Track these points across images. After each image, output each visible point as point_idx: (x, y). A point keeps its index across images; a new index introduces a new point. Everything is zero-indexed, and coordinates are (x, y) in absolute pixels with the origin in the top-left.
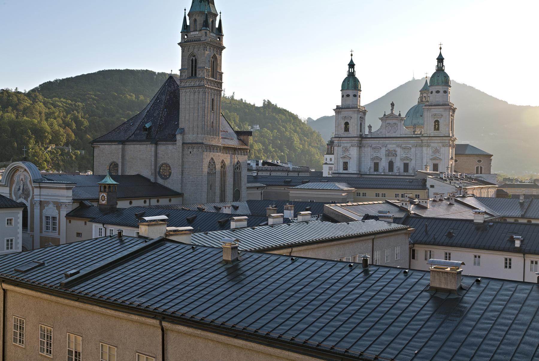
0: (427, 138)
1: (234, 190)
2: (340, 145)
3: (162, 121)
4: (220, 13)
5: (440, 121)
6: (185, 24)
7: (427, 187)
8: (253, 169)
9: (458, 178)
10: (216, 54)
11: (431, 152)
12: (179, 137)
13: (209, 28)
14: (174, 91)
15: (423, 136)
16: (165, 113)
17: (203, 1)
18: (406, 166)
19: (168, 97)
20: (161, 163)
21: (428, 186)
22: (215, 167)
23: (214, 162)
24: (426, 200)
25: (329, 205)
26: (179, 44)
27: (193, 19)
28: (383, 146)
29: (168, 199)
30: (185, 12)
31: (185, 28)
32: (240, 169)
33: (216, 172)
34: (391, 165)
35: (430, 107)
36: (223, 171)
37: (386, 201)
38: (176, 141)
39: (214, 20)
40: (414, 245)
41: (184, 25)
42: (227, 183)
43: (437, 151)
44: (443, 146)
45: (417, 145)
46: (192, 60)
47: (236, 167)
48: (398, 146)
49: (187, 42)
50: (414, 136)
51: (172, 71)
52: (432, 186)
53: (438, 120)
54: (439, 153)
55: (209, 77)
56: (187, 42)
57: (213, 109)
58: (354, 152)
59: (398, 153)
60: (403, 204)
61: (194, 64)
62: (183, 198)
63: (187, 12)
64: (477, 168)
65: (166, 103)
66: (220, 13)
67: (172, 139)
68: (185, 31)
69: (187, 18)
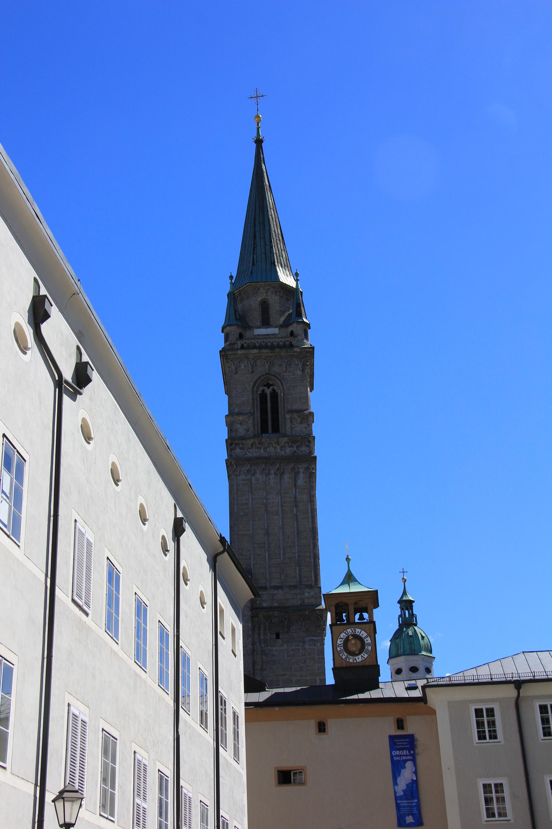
27: (259, 299)
31: (238, 317)
46: (263, 396)
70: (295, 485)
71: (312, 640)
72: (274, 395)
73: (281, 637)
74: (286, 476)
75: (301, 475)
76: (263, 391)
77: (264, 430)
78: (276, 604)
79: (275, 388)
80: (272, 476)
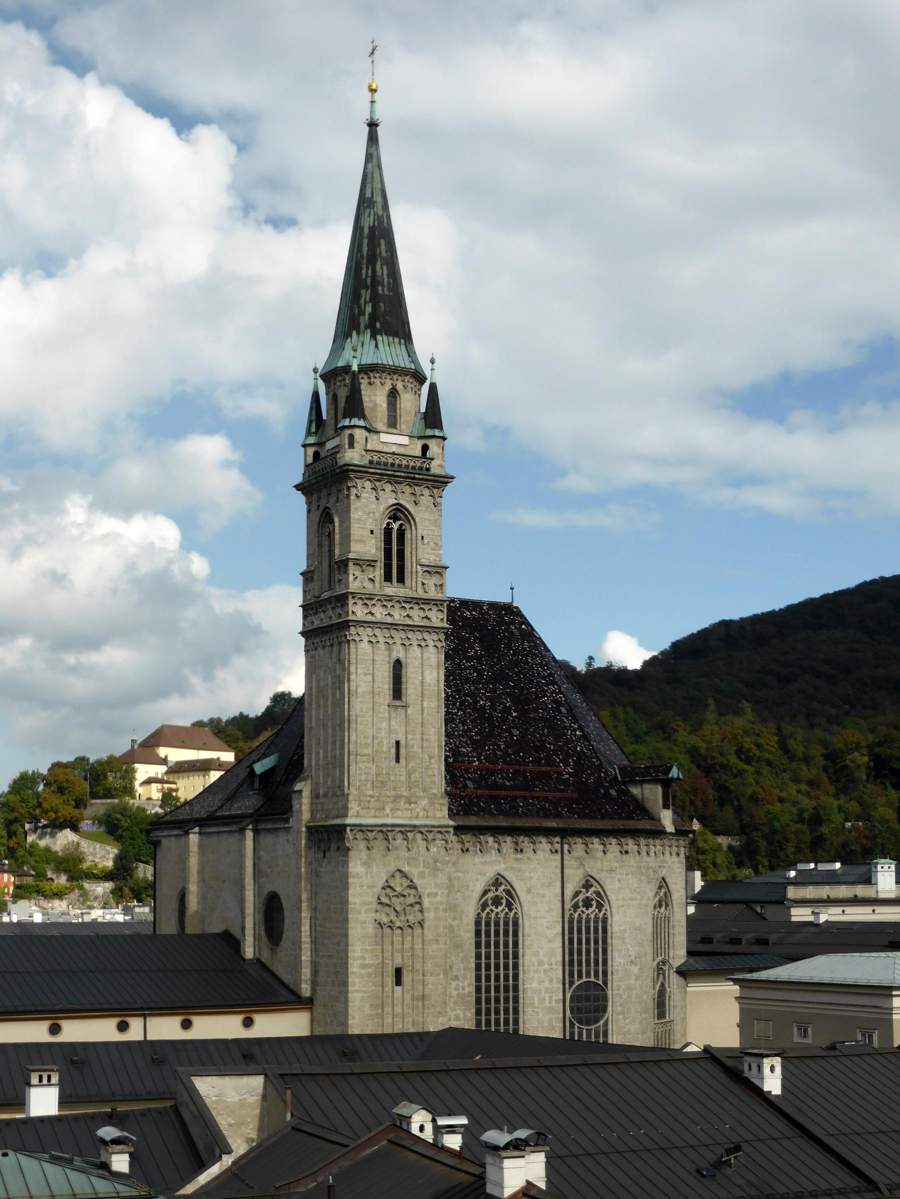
4: (432, 361)
8: (882, 896)
13: (363, 416)
17: (354, 334)
20: (266, 893)
23: (412, 886)
26: (298, 487)
29: (237, 1020)
31: (313, 429)
32: (600, 906)
36: (502, 915)
39: (400, 386)
42: (618, 959)
47: (581, 897)
57: (397, 692)
62: (312, 1014)
66: (432, 361)
68: (312, 440)
74: (335, 648)
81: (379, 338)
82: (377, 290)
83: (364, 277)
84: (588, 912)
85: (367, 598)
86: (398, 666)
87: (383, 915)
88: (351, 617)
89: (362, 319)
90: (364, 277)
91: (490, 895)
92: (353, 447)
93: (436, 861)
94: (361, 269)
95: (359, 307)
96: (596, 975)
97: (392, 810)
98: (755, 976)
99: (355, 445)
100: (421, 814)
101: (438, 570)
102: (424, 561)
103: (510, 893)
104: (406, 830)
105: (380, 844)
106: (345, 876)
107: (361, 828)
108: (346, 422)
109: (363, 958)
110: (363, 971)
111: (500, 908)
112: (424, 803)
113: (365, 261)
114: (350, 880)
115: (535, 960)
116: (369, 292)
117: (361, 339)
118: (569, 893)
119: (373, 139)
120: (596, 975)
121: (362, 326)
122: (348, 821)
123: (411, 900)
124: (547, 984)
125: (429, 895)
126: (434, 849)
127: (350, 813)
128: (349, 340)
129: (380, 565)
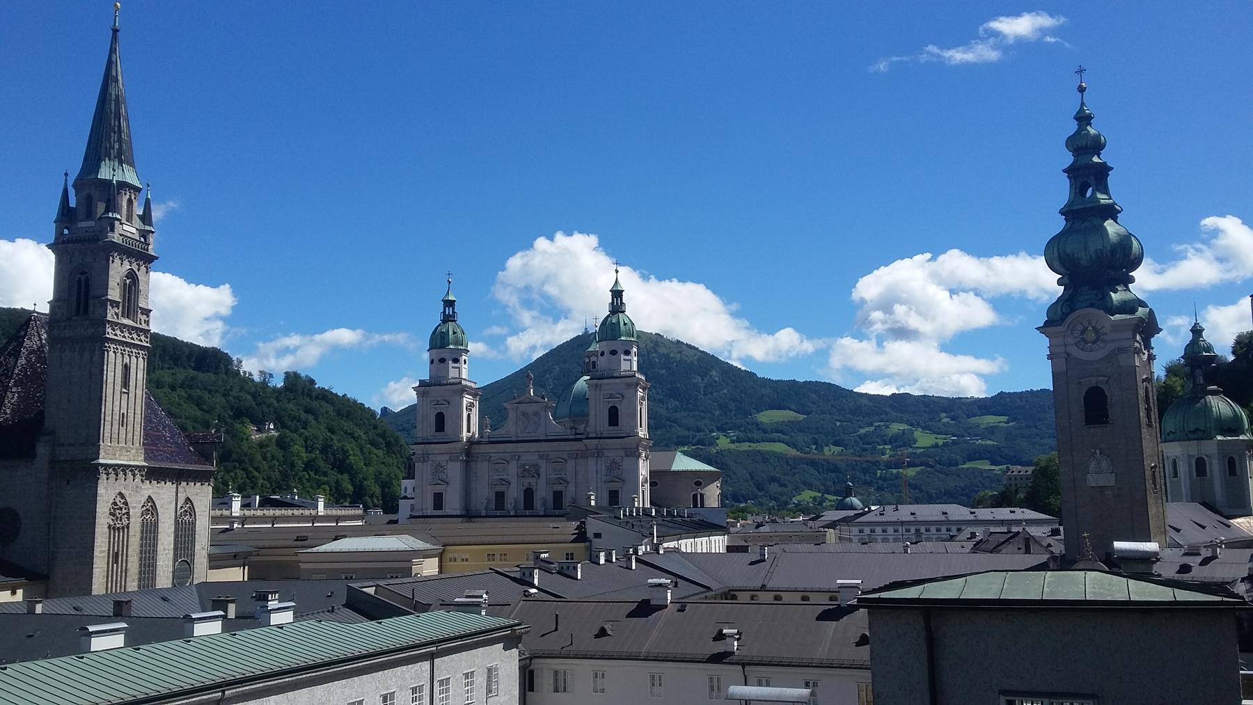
0: (595, 442)
1: (175, 561)
2: (426, 458)
3: (6, 414)
5: (619, 409)
6: (66, 205)
7: (587, 536)
9: (651, 516)
10: (136, 270)
11: (603, 467)
12: (42, 450)
13: (118, 213)
14: (39, 348)
15: (587, 438)
16: (13, 395)
17: (107, 158)
18: (558, 496)
19: (24, 362)
21: (590, 535)
22: (128, 513)
23: (126, 503)
24: (575, 565)
25: (359, 585)
27: (84, 194)
28: (511, 459)
30: (66, 180)
33: (131, 525)
34: (529, 494)
35: (600, 381)
37: (490, 569)
38: (34, 456)
39: (133, 197)
40: (530, 661)
41: (63, 208)
43: (614, 466)
44: (627, 456)
45: (577, 455)
46: (79, 281)
48: (541, 457)
49: (68, 242)
50: (571, 437)
51: (35, 305)
52: (598, 535)
53: (617, 405)
54: (619, 469)
55: (118, 319)
56: (68, 242)
58: (455, 471)
59: (542, 471)
60: (524, 574)
61: (83, 290)
63: (71, 180)
64: (695, 497)
65: (18, 375)
67: (27, 453)
69: (72, 192)
70: (92, 361)
71: (91, 486)
72: (87, 280)
73: (71, 483)
74: (87, 355)
75: (97, 352)
76: (80, 277)
77: (78, 313)
78: (69, 458)
79: (89, 276)
80: (76, 353)
81: (124, 165)
82: (121, 136)
83: (113, 125)
84: (185, 519)
85: (114, 325)
86: (126, 368)
87: (111, 520)
88: (107, 336)
89: (112, 151)
90: (113, 125)
91: (145, 508)
92: (114, 231)
93: (137, 487)
94: (111, 120)
95: (110, 143)
96: (188, 556)
97: (119, 455)
98: (315, 550)
99: (116, 230)
100: (132, 458)
101: (147, 312)
102: (140, 305)
103: (154, 506)
104: (125, 468)
105: (113, 476)
106: (96, 494)
107: (106, 466)
108: (110, 215)
109: (101, 546)
110: (100, 555)
111: (149, 516)
112: (133, 451)
113: (113, 115)
114: (98, 498)
115: (162, 548)
116: (116, 135)
117: (112, 163)
118: (179, 508)
119: (115, 39)
120: (188, 556)
121: (112, 156)
122: (101, 461)
123: (124, 511)
124: (166, 562)
125: (133, 507)
126: (136, 480)
127: (100, 456)
128: (103, 162)
129: (121, 304)
